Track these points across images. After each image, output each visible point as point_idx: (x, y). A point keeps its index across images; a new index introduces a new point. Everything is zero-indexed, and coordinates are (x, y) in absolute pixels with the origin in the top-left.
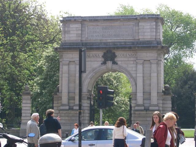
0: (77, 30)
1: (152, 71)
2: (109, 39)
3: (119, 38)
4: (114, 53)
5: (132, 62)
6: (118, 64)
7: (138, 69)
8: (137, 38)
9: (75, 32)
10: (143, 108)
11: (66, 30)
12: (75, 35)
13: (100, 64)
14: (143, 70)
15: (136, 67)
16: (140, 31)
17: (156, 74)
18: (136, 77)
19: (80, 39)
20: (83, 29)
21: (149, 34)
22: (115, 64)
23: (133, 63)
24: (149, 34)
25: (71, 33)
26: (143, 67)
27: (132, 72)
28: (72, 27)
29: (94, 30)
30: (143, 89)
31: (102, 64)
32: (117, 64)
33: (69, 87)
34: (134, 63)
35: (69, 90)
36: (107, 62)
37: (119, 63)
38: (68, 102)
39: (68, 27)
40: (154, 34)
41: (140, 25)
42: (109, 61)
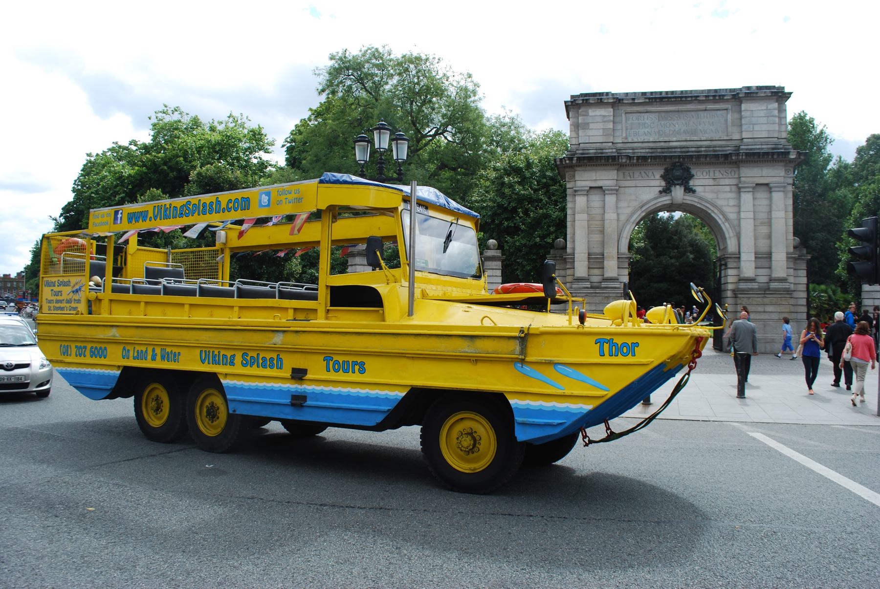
0: (604, 122)
2: (674, 139)
3: (696, 138)
4: (688, 170)
5: (727, 188)
6: (697, 192)
8: (736, 136)
9: (601, 126)
11: (580, 121)
12: (601, 132)
14: (754, 205)
15: (739, 198)
16: (743, 122)
18: (739, 219)
20: (617, 119)
21: (765, 127)
22: (689, 192)
23: (729, 190)
24: (765, 127)
25: (590, 128)
26: (754, 199)
27: (726, 210)
29: (640, 121)
31: (660, 192)
32: (694, 192)
34: (731, 189)
36: (673, 188)
37: (698, 189)
39: (584, 115)
41: (743, 109)
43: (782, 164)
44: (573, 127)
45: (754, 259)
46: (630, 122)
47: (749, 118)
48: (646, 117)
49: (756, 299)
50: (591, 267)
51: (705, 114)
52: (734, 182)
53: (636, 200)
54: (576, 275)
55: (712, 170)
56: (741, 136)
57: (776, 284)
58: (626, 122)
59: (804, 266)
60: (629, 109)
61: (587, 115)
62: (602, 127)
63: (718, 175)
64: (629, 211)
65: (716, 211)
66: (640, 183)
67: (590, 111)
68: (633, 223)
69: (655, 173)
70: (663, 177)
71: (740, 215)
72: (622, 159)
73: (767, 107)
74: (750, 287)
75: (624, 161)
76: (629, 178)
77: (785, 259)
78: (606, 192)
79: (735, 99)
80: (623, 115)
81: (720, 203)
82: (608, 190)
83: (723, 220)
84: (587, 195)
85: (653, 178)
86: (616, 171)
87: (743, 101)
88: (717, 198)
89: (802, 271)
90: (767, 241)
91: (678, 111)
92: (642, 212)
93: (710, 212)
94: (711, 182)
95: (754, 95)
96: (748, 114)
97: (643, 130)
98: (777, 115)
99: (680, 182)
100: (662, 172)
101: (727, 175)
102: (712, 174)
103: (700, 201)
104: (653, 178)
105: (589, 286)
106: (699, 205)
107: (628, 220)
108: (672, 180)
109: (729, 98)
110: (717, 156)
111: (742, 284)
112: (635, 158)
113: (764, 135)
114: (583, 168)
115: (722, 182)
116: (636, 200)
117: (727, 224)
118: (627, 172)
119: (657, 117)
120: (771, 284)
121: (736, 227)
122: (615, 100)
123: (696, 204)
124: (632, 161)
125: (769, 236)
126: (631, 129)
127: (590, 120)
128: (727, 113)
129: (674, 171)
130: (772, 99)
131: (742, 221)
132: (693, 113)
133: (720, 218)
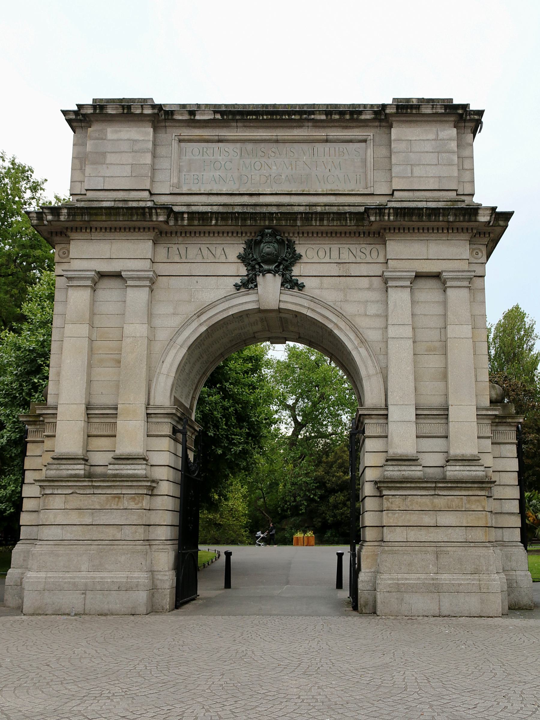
4: (291, 245)
5: (365, 282)
9: (128, 158)
12: (127, 170)
16: (394, 161)
21: (433, 171)
22: (292, 288)
23: (368, 286)
24: (433, 171)
26: (413, 302)
27: (362, 323)
29: (206, 157)
31: (237, 287)
32: (301, 287)
33: (89, 382)
34: (371, 284)
35: (89, 393)
36: (260, 279)
38: (86, 444)
41: (393, 137)
42: (269, 276)
43: (467, 236)
44: (77, 161)
46: (187, 157)
49: (419, 499)
51: (327, 149)
52: (377, 270)
53: (190, 301)
54: (56, 451)
55: (335, 248)
56: (391, 186)
57: (458, 468)
58: (180, 158)
59: (512, 437)
60: (187, 133)
61: (103, 139)
62: (130, 161)
63: (346, 256)
64: (175, 322)
65: (342, 324)
70: (243, 258)
71: (387, 332)
74: (406, 474)
75: (161, 218)
77: (475, 418)
78: (129, 283)
79: (381, 121)
80: (175, 144)
81: (349, 309)
82: (132, 278)
86: (150, 243)
87: (394, 125)
88: (346, 301)
89: (508, 447)
90: (441, 385)
92: (200, 325)
93: (330, 326)
94: (334, 270)
95: (414, 111)
98: (455, 149)
99: (273, 267)
100: (240, 249)
102: (335, 254)
103: (312, 305)
104: (223, 259)
105: (82, 472)
106: (310, 314)
108: (259, 264)
109: (368, 117)
110: (340, 216)
111: (391, 468)
112: (186, 216)
114: (87, 236)
115: (354, 270)
117: (363, 351)
118: (175, 247)
119: (238, 151)
120: (449, 468)
121: (381, 357)
122: (156, 111)
123: (304, 311)
126: (189, 171)
129: (262, 245)
130: (446, 121)
131: (390, 342)
132: (305, 146)
133: (350, 339)
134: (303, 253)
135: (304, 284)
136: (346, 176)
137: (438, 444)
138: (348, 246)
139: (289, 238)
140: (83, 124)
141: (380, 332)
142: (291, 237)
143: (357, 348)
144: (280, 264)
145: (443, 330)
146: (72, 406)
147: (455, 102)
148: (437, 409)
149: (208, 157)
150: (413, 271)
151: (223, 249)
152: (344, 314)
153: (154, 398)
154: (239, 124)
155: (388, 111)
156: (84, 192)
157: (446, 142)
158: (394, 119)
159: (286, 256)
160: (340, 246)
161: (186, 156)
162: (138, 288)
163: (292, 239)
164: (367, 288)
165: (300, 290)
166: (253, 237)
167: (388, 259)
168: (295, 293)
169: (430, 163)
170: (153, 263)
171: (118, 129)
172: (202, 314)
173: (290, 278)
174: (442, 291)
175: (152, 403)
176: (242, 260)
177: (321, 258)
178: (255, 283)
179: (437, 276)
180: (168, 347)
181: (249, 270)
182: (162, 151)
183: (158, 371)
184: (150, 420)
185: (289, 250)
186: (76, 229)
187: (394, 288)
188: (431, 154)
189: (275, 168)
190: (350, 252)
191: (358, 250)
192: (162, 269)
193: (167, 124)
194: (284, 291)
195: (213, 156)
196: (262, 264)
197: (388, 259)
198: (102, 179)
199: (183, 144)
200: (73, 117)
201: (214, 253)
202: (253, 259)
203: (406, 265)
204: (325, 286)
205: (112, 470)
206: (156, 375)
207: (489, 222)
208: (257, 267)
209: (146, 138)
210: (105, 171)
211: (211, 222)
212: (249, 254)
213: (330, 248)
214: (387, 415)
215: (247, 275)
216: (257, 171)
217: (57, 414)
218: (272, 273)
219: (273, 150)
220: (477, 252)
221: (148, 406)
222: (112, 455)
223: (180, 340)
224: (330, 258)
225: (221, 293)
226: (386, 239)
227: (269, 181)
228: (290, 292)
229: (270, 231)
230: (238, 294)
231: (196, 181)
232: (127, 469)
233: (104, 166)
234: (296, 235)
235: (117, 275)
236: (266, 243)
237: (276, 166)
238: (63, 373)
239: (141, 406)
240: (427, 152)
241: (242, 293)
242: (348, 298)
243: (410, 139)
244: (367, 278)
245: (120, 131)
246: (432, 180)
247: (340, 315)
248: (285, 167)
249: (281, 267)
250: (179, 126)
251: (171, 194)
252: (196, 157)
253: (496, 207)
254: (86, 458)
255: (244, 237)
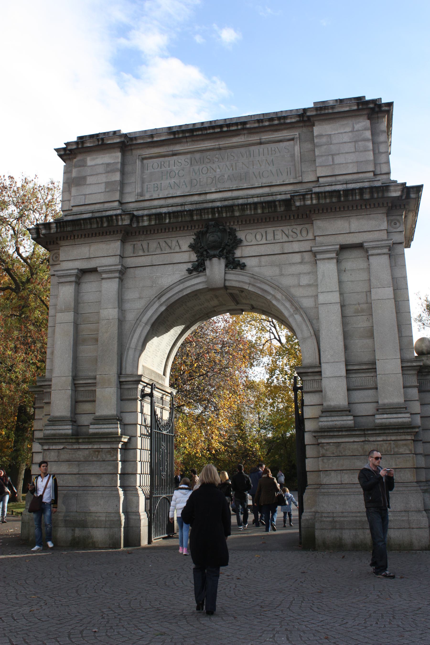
0: (108, 172)
1: (373, 281)
4: (232, 232)
5: (297, 258)
6: (247, 268)
7: (320, 277)
9: (103, 179)
10: (348, 421)
12: (102, 188)
13: (184, 273)
14: (340, 282)
15: (314, 273)
16: (317, 153)
17: (389, 292)
18: (316, 307)
19: (117, 197)
21: (351, 158)
22: (235, 268)
23: (299, 260)
24: (351, 158)
26: (339, 271)
27: (297, 292)
28: (93, 163)
30: (346, 348)
31: (190, 271)
32: (243, 266)
34: (303, 259)
36: (207, 263)
37: (248, 262)
39: (80, 166)
40: (370, 156)
41: (315, 134)
42: (215, 260)
44: (66, 185)
45: (344, 373)
46: (149, 171)
47: (325, 147)
48: (172, 162)
50: (81, 399)
51: (261, 150)
52: (306, 246)
54: (52, 414)
55: (270, 230)
56: (316, 174)
58: (143, 172)
61: (83, 164)
62: (104, 180)
63: (279, 236)
64: (140, 305)
65: (279, 296)
66: (156, 260)
67: (89, 159)
68: (146, 324)
69: (181, 242)
72: (122, 220)
73: (353, 127)
76: (141, 253)
78: (104, 276)
79: (303, 121)
80: (138, 163)
83: (292, 311)
84: (78, 283)
85: (177, 249)
86: (119, 243)
87: (316, 123)
88: (282, 275)
91: (220, 149)
92: (161, 305)
93: (269, 298)
96: (324, 140)
97: (168, 182)
98: (370, 137)
99: (217, 252)
101: (295, 236)
102: (270, 237)
104: (177, 249)
105: (70, 432)
107: (138, 320)
108: (206, 250)
109: (293, 120)
113: (352, 169)
115: (288, 248)
116: (152, 286)
118: (139, 243)
119: (189, 161)
122: (123, 139)
123: (246, 287)
124: (141, 224)
125: (370, 334)
127: (88, 171)
128: (294, 146)
129: (208, 235)
130: (361, 115)
132: (243, 150)
133: (286, 307)
134: (243, 238)
135: (246, 264)
136: (278, 171)
137: (368, 395)
138: (281, 228)
139: (231, 227)
140: (70, 157)
141: (313, 299)
142: (232, 225)
143: (292, 315)
144: (224, 249)
145: (368, 294)
146: (63, 378)
147: (367, 98)
148: (365, 364)
149: (165, 169)
150: (337, 245)
151: (177, 241)
152: (281, 286)
153: (126, 368)
154: (188, 140)
155: (308, 114)
156: (71, 208)
157: (361, 132)
158: (315, 119)
159: (228, 242)
160: (274, 229)
161: (147, 170)
162: (111, 280)
163: (233, 227)
164: (300, 263)
165: (241, 269)
166: (201, 228)
167: (315, 236)
168: (238, 272)
169: (349, 151)
170: (122, 258)
171: (95, 157)
172: (162, 296)
173: (232, 260)
174: (366, 259)
175: (123, 372)
176: (192, 249)
177: (259, 240)
178: (204, 267)
179: (360, 246)
180: (135, 326)
181: (199, 256)
182: (129, 168)
183: (128, 346)
184: (123, 387)
185: (231, 237)
186: (65, 238)
187: (321, 261)
188: (350, 144)
189: (219, 170)
190: (283, 233)
191: (290, 231)
192: (130, 262)
193: (132, 148)
194: (228, 271)
195: (169, 167)
196: (208, 251)
197: (315, 236)
198: (83, 197)
199: (145, 161)
200: (62, 153)
201: (170, 245)
202: (201, 247)
203: (331, 240)
204: (263, 264)
205: (93, 429)
206: (126, 349)
207: (401, 196)
208: (205, 253)
209: (116, 161)
210: (87, 190)
211: (165, 221)
212: (198, 243)
213: (266, 232)
214: (321, 372)
215: (197, 261)
216: (204, 175)
217: (51, 385)
218: (217, 257)
219: (217, 156)
220: (395, 222)
221: (120, 374)
222: (92, 417)
223: (145, 319)
224: (266, 240)
225: (177, 277)
226: (313, 219)
227: (214, 182)
228: (233, 272)
229: (213, 223)
230: (190, 278)
231: (156, 189)
232: (104, 428)
233: (85, 186)
234: (236, 223)
235: (94, 271)
236: (210, 233)
237: (219, 168)
238: (55, 352)
239: (114, 376)
240: (345, 143)
241: (193, 276)
242: (283, 273)
243: (330, 133)
244: (300, 254)
245: (97, 158)
246: (351, 166)
247: (277, 288)
248: (227, 169)
249: (225, 251)
250: (142, 148)
251: (136, 201)
252: (156, 170)
253: (405, 183)
254: (74, 420)
255: (194, 229)
